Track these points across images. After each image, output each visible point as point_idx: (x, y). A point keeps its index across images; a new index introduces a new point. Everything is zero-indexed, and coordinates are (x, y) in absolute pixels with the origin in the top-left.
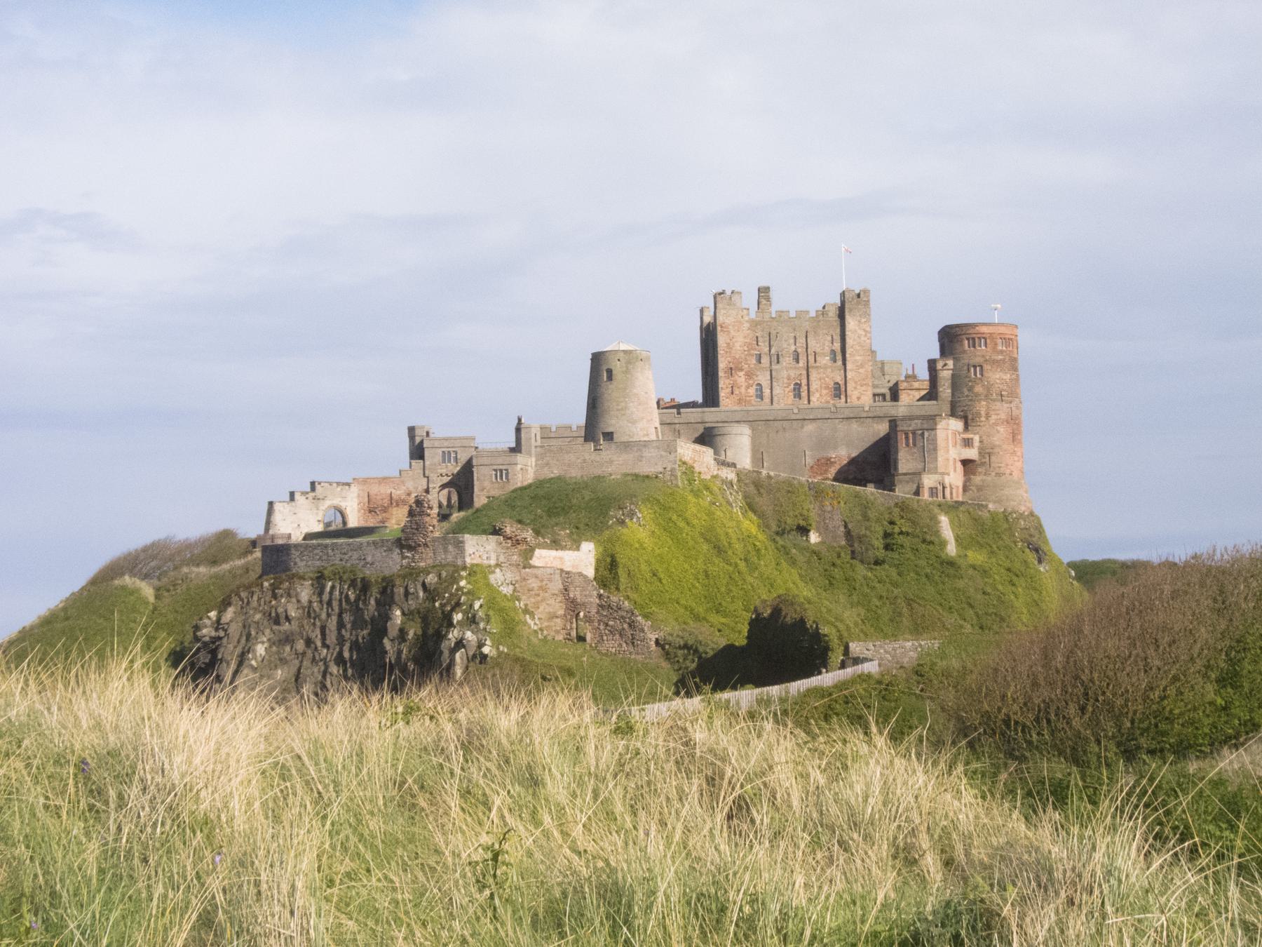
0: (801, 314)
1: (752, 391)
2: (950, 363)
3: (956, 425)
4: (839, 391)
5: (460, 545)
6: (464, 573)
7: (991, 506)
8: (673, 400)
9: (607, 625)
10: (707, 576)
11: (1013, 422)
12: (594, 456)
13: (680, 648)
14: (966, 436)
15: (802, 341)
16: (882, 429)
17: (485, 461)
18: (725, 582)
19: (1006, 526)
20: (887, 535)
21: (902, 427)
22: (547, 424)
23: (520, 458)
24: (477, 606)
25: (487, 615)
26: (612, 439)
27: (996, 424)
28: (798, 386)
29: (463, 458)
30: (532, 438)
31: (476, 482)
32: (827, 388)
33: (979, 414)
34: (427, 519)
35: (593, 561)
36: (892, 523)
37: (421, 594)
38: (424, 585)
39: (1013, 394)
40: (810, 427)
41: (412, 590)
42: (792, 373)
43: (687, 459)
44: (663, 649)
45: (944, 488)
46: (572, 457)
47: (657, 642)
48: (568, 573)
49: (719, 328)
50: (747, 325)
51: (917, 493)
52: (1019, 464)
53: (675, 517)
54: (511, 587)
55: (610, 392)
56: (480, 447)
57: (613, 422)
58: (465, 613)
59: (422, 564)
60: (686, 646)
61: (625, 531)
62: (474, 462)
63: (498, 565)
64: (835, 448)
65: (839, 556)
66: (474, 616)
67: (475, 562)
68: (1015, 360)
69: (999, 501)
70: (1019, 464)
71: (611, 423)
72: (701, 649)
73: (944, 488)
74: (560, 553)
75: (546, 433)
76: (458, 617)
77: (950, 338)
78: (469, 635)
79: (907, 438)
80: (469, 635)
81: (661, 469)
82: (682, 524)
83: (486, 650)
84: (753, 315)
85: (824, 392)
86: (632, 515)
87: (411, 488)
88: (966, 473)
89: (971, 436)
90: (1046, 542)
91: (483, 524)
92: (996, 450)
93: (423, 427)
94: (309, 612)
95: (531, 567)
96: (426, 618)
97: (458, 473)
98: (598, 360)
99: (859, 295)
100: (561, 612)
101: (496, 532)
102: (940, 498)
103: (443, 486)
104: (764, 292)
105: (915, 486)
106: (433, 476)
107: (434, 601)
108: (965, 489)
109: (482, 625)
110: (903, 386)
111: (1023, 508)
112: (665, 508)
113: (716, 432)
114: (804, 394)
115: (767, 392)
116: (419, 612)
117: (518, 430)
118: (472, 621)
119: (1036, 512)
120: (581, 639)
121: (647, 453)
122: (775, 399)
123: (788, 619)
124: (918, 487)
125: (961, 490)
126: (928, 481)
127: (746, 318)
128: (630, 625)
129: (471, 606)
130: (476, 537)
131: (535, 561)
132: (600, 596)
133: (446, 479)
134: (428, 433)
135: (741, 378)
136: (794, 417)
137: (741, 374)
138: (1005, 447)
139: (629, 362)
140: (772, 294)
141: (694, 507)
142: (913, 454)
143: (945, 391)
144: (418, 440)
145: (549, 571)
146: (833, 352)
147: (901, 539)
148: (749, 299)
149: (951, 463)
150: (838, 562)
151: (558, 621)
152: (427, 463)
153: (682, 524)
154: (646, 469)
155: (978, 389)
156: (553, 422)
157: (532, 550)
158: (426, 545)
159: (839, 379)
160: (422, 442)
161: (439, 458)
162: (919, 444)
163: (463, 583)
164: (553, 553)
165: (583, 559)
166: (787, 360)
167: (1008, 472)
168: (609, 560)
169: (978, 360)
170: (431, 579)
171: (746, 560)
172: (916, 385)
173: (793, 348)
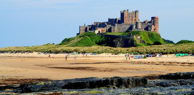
11: (158, 25)
16: (147, 26)
94: (122, 40)
126: (151, 31)
143: (152, 22)
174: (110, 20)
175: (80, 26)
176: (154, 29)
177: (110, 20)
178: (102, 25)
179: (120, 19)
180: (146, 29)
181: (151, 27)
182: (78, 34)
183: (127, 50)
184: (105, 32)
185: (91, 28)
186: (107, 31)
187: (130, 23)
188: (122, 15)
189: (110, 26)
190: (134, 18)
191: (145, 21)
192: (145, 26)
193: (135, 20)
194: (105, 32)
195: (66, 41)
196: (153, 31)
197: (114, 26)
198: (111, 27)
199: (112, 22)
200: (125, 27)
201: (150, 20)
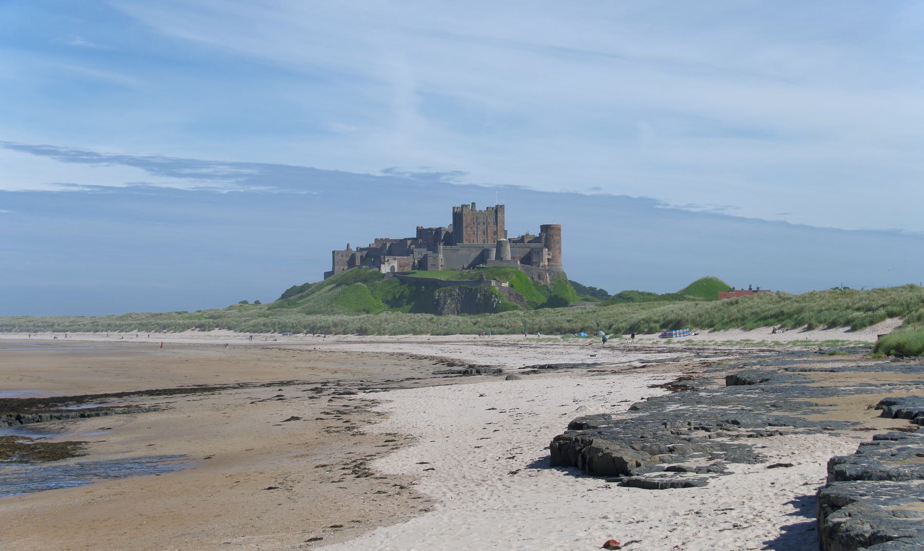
11: (560, 249)
16: (528, 250)
96: (484, 295)
104: (473, 204)
126: (541, 264)
135: (469, 229)
143: (543, 241)
174: (420, 231)
175: (334, 252)
176: (549, 260)
177: (420, 231)
178: (398, 248)
179: (451, 231)
180: (527, 260)
181: (539, 253)
182: (327, 275)
183: (475, 324)
184: (409, 269)
185: (367, 255)
186: (414, 267)
187: (481, 243)
188: (458, 216)
189: (424, 251)
190: (492, 228)
191: (523, 237)
192: (524, 252)
193: (495, 233)
194: (409, 269)
195: (294, 295)
196: (546, 263)
197: (435, 251)
198: (425, 257)
199: (429, 238)
200: (465, 253)
201: (536, 232)
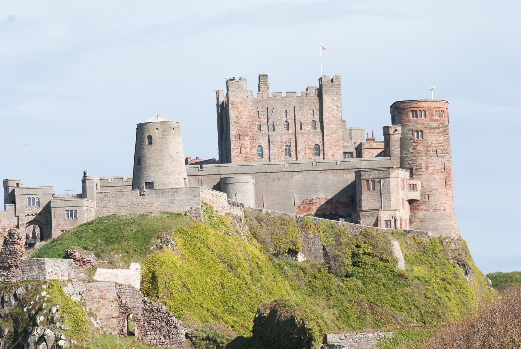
0: (290, 94)
1: (255, 151)
2: (399, 129)
3: (405, 174)
4: (319, 150)
5: (41, 266)
6: (44, 287)
7: (430, 234)
8: (197, 158)
9: (150, 323)
10: (223, 287)
11: (446, 171)
12: (140, 200)
13: (203, 339)
14: (412, 182)
15: (291, 114)
16: (351, 177)
17: (60, 204)
18: (236, 291)
19: (441, 248)
20: (354, 255)
21: (365, 176)
22: (105, 176)
23: (85, 202)
24: (54, 310)
25: (62, 317)
26: (152, 187)
27: (433, 173)
28: (288, 147)
29: (44, 203)
30: (93, 187)
31: (53, 220)
32: (310, 148)
33: (420, 166)
34: (17, 247)
35: (139, 276)
36: (358, 246)
37: (13, 302)
38: (15, 295)
39: (446, 152)
40: (297, 177)
41: (6, 300)
42: (285, 138)
43: (207, 201)
44: (191, 340)
45: (395, 220)
46: (123, 200)
47: (187, 335)
48: (121, 285)
49: (230, 105)
50: (251, 103)
51: (376, 224)
52: (450, 203)
53: (199, 244)
54: (79, 296)
55: (151, 153)
56: (56, 195)
57: (153, 174)
58: (46, 315)
59: (14, 280)
60: (208, 338)
61: (162, 254)
62: (52, 206)
63: (70, 280)
64: (316, 192)
65: (319, 271)
66: (52, 318)
67: (53, 278)
68: (446, 127)
69: (435, 230)
70: (450, 203)
71: (150, 176)
72: (219, 340)
73: (395, 220)
74: (115, 271)
75: (105, 184)
76: (40, 319)
77: (399, 110)
78: (48, 332)
79: (368, 184)
80: (48, 332)
81: (189, 209)
82: (204, 249)
83: (61, 343)
84: (255, 96)
85: (308, 151)
86: (167, 242)
87: (6, 225)
88: (411, 210)
89: (414, 182)
90: (470, 259)
91: (58, 250)
92: (433, 192)
93: (14, 180)
95: (94, 281)
97: (40, 213)
98: (141, 128)
99: (332, 81)
100: (116, 314)
101: (68, 256)
102: (393, 228)
103: (30, 223)
104: (263, 79)
105: (374, 220)
106: (22, 216)
107: (23, 307)
108: (411, 221)
109: (58, 324)
110: (365, 146)
111: (453, 235)
112: (192, 237)
113: (229, 181)
114: (293, 153)
115: (266, 152)
116: (12, 316)
117: (84, 181)
118: (51, 321)
119: (463, 238)
120: (131, 334)
121: (177, 197)
122: (272, 156)
123: (282, 318)
124: (377, 220)
125: (408, 222)
126: (384, 216)
127: (250, 98)
128: (167, 324)
129: (50, 310)
130: (53, 260)
131: (96, 277)
132: (144, 302)
133: (31, 218)
134: (18, 184)
135: (246, 142)
136: (285, 170)
137: (247, 138)
138: (440, 190)
139: (164, 131)
140: (270, 80)
141: (213, 236)
142: (372, 196)
143: (396, 149)
144: (10, 189)
145: (108, 284)
146: (314, 122)
147: (365, 258)
148: (253, 84)
149: (401, 202)
150: (319, 276)
151: (114, 320)
152: (17, 206)
153: (204, 249)
154: (177, 209)
155: (420, 148)
156: (110, 176)
157: (94, 269)
158: (16, 266)
159: (319, 142)
160: (13, 191)
161: (26, 202)
162: (378, 188)
163: (44, 294)
164: (110, 271)
165: (132, 275)
166: (280, 128)
167: (442, 208)
168: (151, 275)
169: (420, 127)
170: (21, 291)
171: (251, 275)
172: (375, 145)
173: (285, 119)
181: (379, 182)
